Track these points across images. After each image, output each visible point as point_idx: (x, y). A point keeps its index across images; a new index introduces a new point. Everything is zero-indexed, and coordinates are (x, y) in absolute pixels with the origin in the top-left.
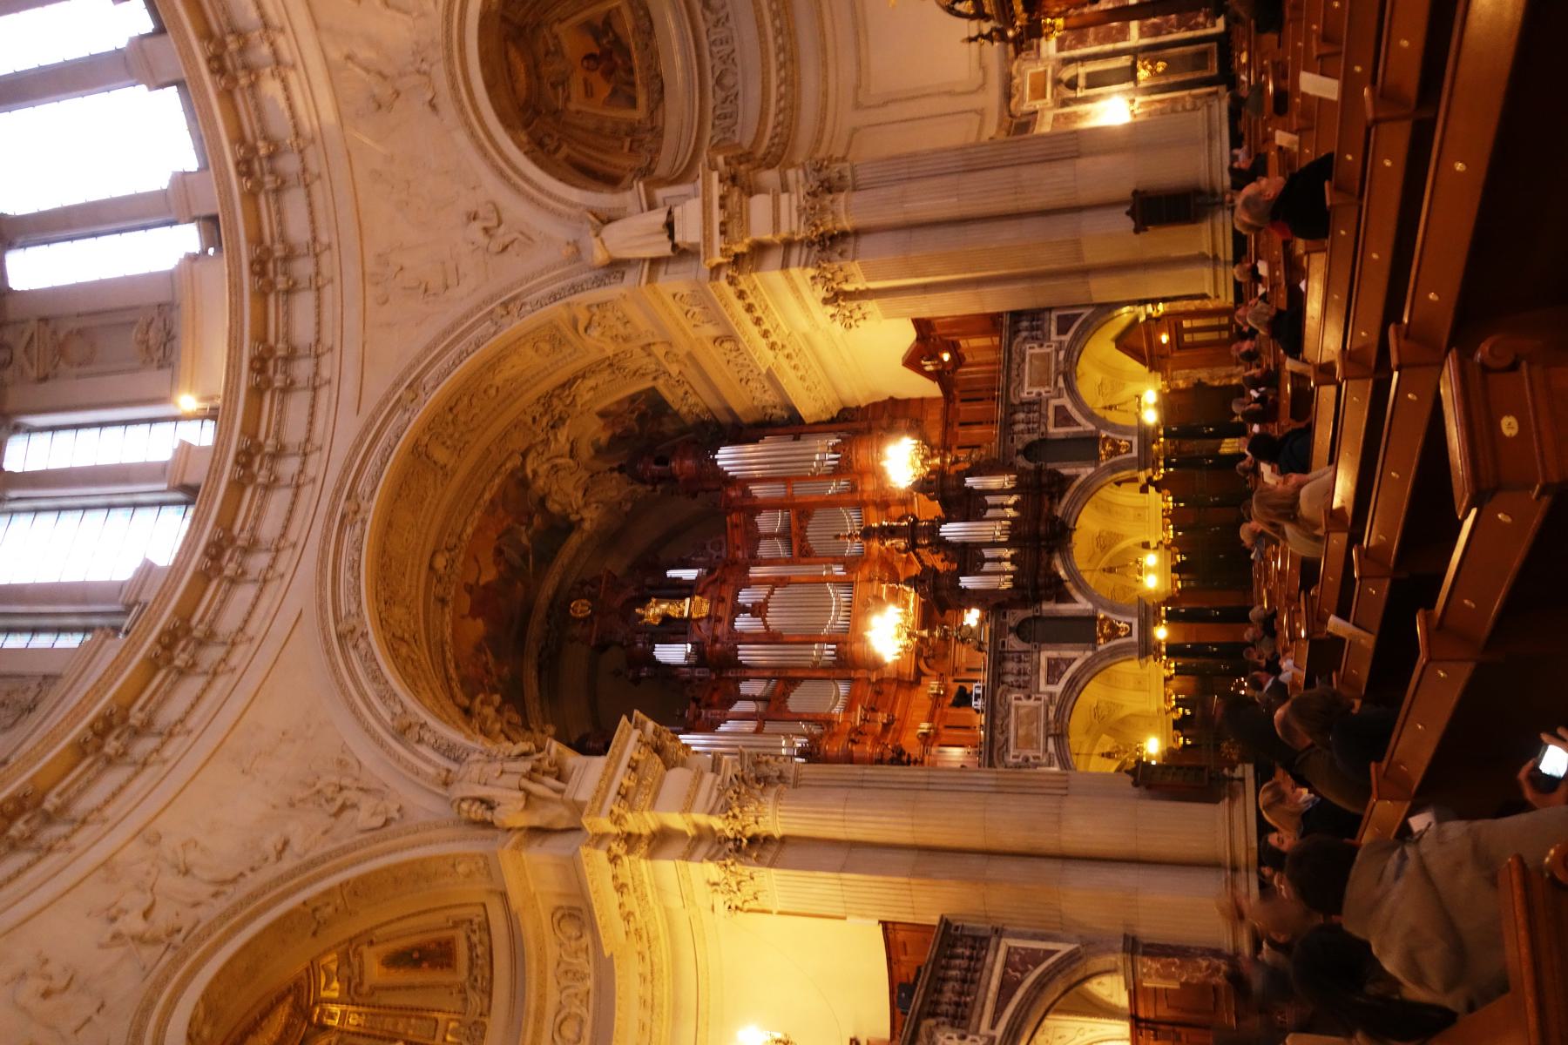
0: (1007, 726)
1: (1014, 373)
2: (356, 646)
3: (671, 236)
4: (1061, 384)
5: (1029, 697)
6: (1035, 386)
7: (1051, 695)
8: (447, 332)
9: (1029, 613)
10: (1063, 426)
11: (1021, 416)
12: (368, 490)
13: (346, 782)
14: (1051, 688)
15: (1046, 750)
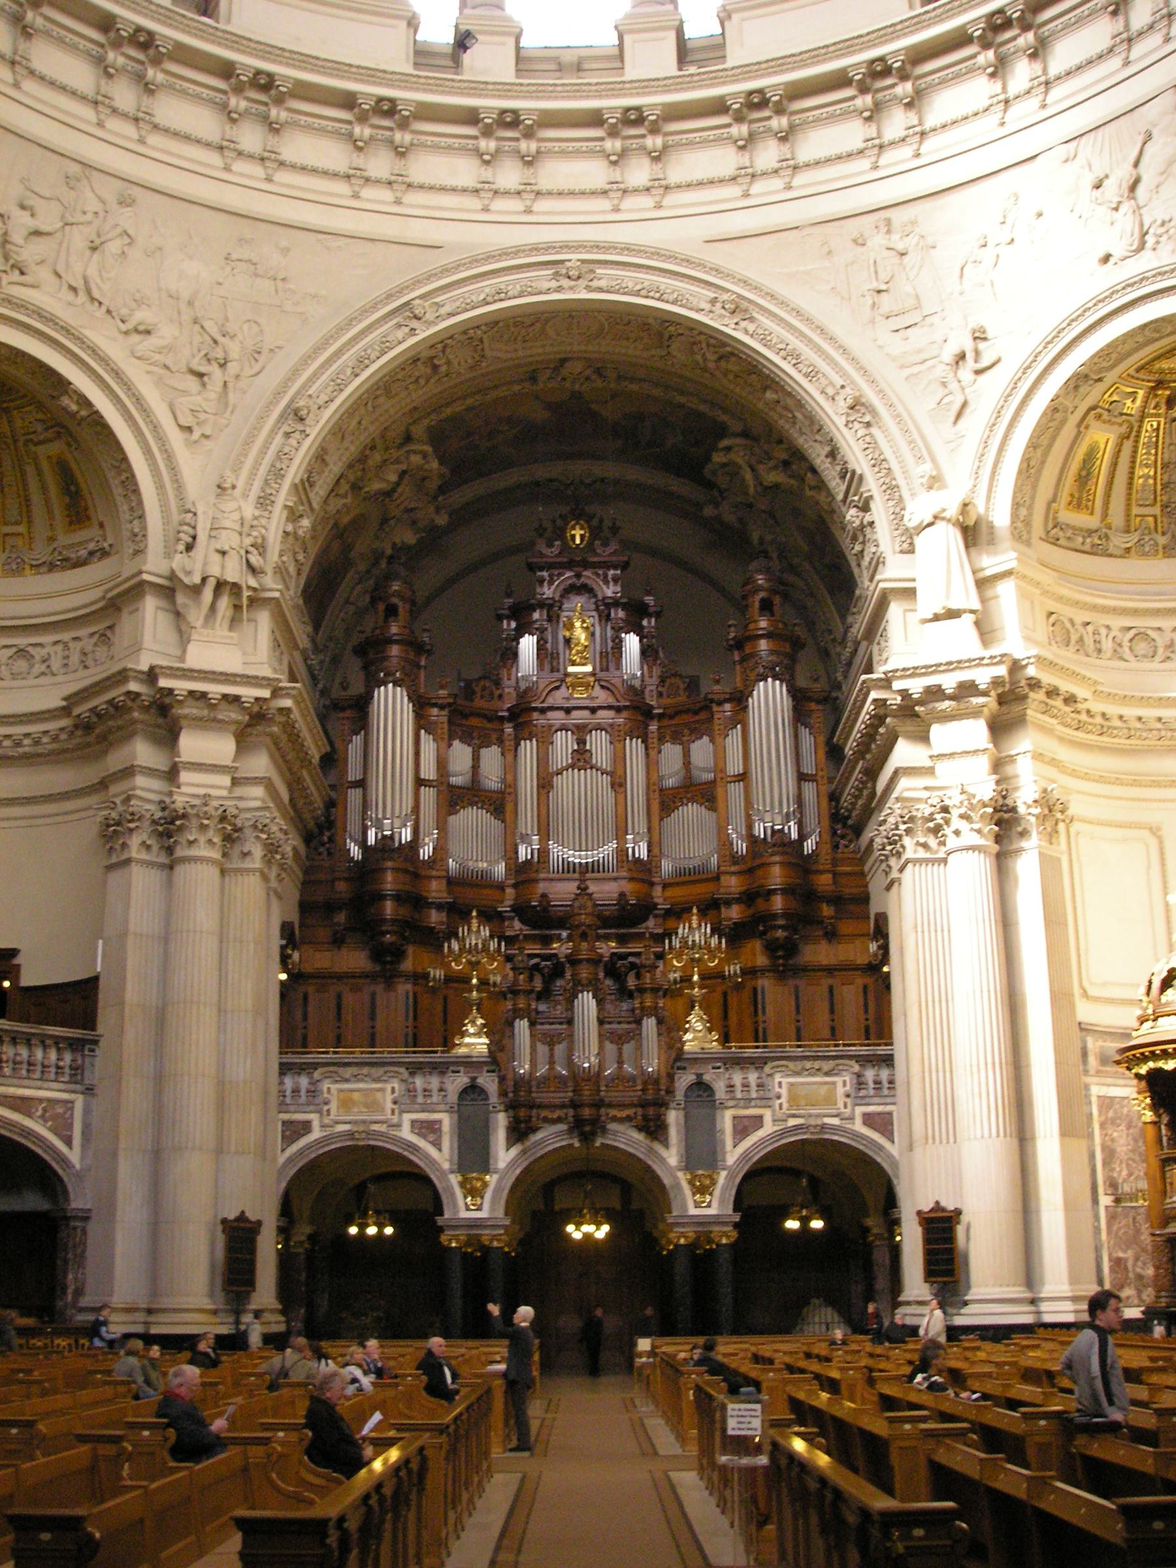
0: (362, 1080)
1: (808, 1064)
2: (399, 326)
3: (937, 618)
4: (792, 1122)
5: (395, 1103)
6: (789, 1091)
7: (398, 1126)
8: (822, 331)
9: (494, 1099)
10: (734, 1126)
11: (753, 1077)
12: (602, 283)
13: (232, 368)
14: (406, 1126)
15: (337, 1123)
